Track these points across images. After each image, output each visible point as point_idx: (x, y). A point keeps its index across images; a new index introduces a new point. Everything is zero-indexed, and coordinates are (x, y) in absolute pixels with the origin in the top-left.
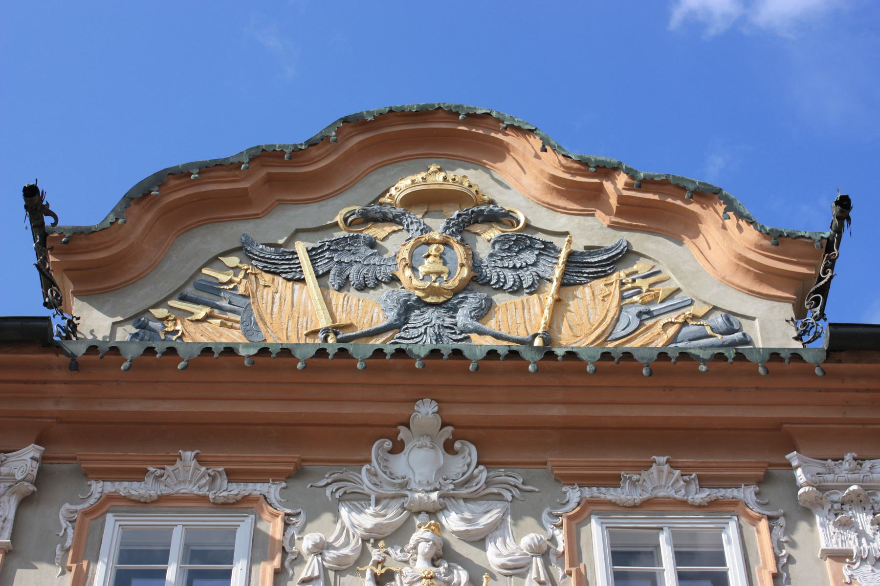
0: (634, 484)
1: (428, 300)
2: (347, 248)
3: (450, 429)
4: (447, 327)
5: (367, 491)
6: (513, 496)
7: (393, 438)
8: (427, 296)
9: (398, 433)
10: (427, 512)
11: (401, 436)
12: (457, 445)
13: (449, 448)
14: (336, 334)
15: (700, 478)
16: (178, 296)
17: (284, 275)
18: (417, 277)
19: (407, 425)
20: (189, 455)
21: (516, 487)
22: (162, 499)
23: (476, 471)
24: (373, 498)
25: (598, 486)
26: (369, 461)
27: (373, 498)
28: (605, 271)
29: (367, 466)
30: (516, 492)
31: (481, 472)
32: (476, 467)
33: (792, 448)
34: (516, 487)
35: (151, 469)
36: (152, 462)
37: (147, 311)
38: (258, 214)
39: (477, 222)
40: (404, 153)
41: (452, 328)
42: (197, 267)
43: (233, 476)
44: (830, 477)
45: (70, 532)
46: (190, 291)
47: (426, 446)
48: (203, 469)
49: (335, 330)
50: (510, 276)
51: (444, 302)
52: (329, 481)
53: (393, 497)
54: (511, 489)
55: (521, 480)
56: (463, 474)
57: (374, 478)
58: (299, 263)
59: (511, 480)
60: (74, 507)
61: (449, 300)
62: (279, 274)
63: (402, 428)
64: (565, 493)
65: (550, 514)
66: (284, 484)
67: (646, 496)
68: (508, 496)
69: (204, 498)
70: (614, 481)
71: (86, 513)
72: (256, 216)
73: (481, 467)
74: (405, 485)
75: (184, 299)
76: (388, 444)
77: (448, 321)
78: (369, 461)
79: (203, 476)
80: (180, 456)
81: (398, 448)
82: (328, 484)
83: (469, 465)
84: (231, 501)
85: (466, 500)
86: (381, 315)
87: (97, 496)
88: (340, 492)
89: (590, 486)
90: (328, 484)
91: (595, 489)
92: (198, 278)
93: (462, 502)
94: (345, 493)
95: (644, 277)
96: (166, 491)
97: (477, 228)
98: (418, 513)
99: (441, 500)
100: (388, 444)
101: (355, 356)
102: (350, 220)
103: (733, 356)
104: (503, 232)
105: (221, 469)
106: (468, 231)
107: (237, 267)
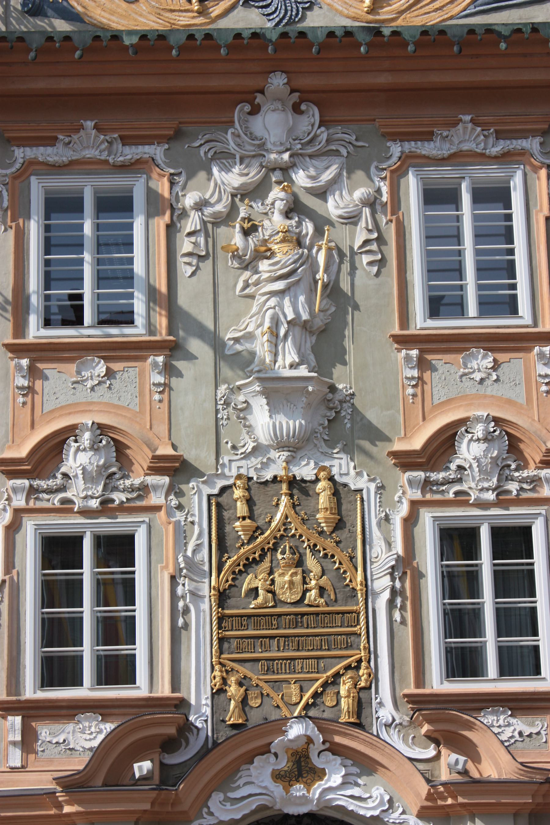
6: (348, 152)
11: (257, 101)
12: (303, 107)
21: (350, 143)
23: (319, 131)
25: (415, 141)
30: (351, 148)
31: (322, 132)
32: (319, 127)
34: (350, 143)
47: (278, 109)
52: (202, 142)
54: (347, 145)
55: (354, 137)
56: (309, 134)
57: (238, 139)
63: (259, 96)
64: (389, 147)
65: (377, 168)
66: (166, 146)
68: (344, 152)
76: (247, 108)
79: (102, 142)
82: (201, 145)
83: (313, 125)
85: (311, 156)
89: (409, 141)
90: (201, 145)
91: (413, 143)
93: (307, 159)
94: (215, 152)
99: (292, 159)
100: (247, 108)
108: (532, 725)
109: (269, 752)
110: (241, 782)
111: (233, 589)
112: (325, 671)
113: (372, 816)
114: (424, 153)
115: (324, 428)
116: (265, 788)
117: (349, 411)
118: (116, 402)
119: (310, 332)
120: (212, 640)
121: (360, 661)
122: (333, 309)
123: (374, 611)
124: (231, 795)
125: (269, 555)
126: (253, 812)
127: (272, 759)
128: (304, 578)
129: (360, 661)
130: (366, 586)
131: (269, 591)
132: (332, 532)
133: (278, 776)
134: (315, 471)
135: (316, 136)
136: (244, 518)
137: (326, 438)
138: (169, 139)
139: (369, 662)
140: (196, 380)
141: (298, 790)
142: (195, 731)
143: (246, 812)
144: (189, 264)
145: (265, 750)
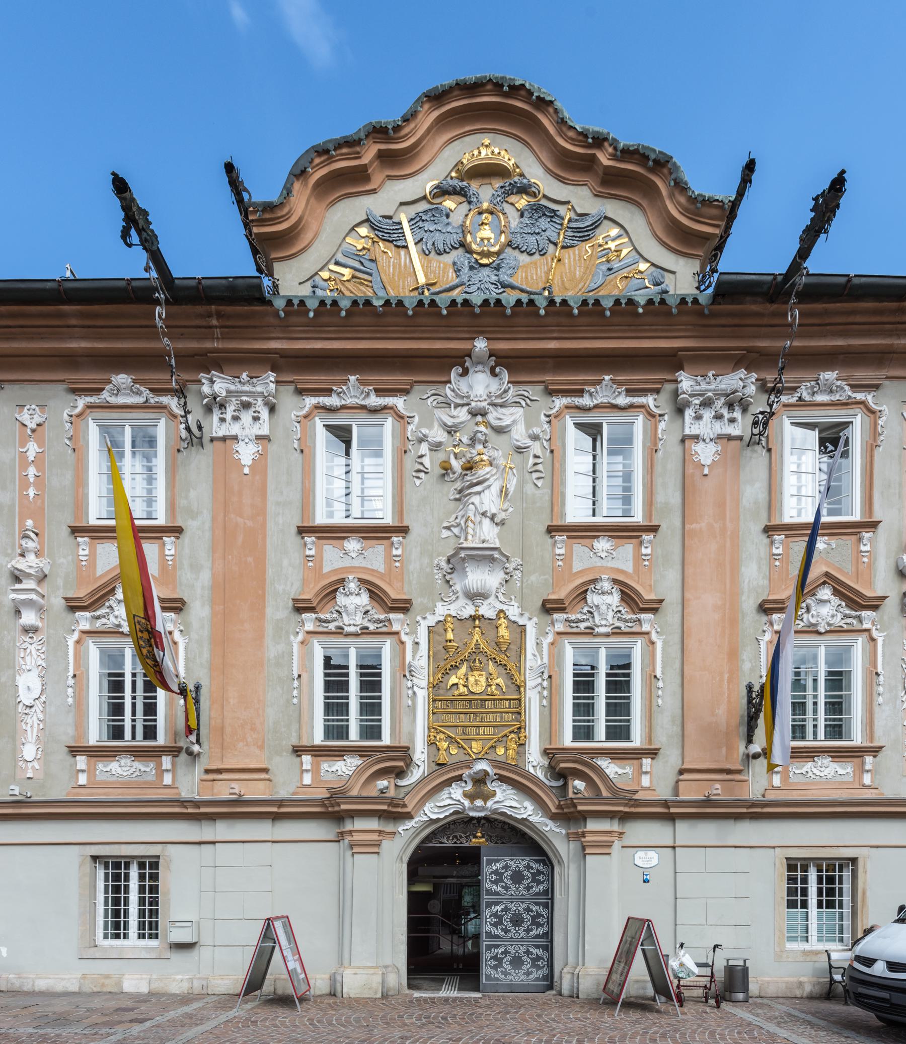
0: (591, 394)
1: (481, 261)
2: (432, 219)
3: (494, 358)
4: (492, 284)
5: (449, 402)
7: (463, 367)
8: (481, 259)
9: (465, 362)
10: (481, 415)
11: (467, 364)
12: (498, 370)
13: (493, 373)
14: (428, 290)
15: (627, 391)
16: (333, 261)
17: (395, 243)
18: (475, 243)
19: (470, 356)
20: (353, 378)
21: (528, 397)
22: (343, 407)
24: (452, 405)
25: (571, 396)
26: (450, 382)
27: (452, 405)
28: (589, 235)
29: (449, 385)
30: (528, 401)
33: (681, 368)
34: (528, 397)
35: (335, 388)
36: (335, 384)
37: (317, 274)
38: (375, 189)
39: (512, 193)
40: (467, 128)
41: (495, 284)
42: (342, 237)
43: (379, 392)
44: (698, 388)
45: (299, 428)
46: (340, 257)
48: (362, 387)
49: (429, 285)
50: (532, 239)
51: (491, 264)
52: (429, 395)
53: (463, 405)
58: (403, 232)
59: (526, 394)
60: (298, 414)
61: (494, 261)
62: (391, 242)
63: (467, 358)
65: (545, 415)
66: (405, 398)
67: (596, 402)
68: (523, 403)
69: (363, 407)
70: (580, 393)
71: (305, 417)
72: (374, 191)
73: (509, 385)
74: (468, 397)
75: (337, 263)
77: (494, 279)
78: (450, 382)
79: (362, 393)
80: (349, 380)
81: (465, 372)
82: (428, 397)
83: (503, 383)
84: (379, 408)
86: (454, 275)
87: (308, 406)
88: (435, 403)
89: (567, 397)
90: (428, 397)
91: (568, 399)
92: (344, 246)
93: (499, 408)
95: (613, 240)
96: (343, 402)
97: (513, 199)
98: (476, 415)
100: (460, 370)
101: (440, 305)
102: (433, 193)
103: (659, 300)
104: (529, 202)
105: (371, 388)
106: (507, 202)
107: (367, 236)
108: (624, 768)
109: (462, 780)
110: (444, 797)
111: (441, 684)
112: (499, 733)
113: (523, 818)
114: (577, 404)
115: (503, 586)
116: (459, 801)
117: (520, 575)
118: (370, 567)
119: (497, 524)
120: (429, 714)
121: (520, 728)
122: (511, 510)
123: (530, 699)
124: (438, 804)
125: (465, 663)
126: (451, 815)
127: (464, 784)
128: (487, 679)
129: (520, 728)
130: (525, 684)
131: (464, 686)
132: (505, 651)
133: (466, 795)
134: (496, 613)
135: (506, 391)
136: (450, 641)
137: (504, 592)
138: (406, 392)
139: (525, 729)
140: (421, 553)
141: (479, 803)
142: (417, 767)
143: (447, 814)
144: (418, 478)
145: (459, 778)
